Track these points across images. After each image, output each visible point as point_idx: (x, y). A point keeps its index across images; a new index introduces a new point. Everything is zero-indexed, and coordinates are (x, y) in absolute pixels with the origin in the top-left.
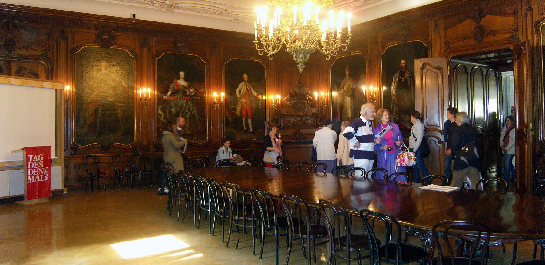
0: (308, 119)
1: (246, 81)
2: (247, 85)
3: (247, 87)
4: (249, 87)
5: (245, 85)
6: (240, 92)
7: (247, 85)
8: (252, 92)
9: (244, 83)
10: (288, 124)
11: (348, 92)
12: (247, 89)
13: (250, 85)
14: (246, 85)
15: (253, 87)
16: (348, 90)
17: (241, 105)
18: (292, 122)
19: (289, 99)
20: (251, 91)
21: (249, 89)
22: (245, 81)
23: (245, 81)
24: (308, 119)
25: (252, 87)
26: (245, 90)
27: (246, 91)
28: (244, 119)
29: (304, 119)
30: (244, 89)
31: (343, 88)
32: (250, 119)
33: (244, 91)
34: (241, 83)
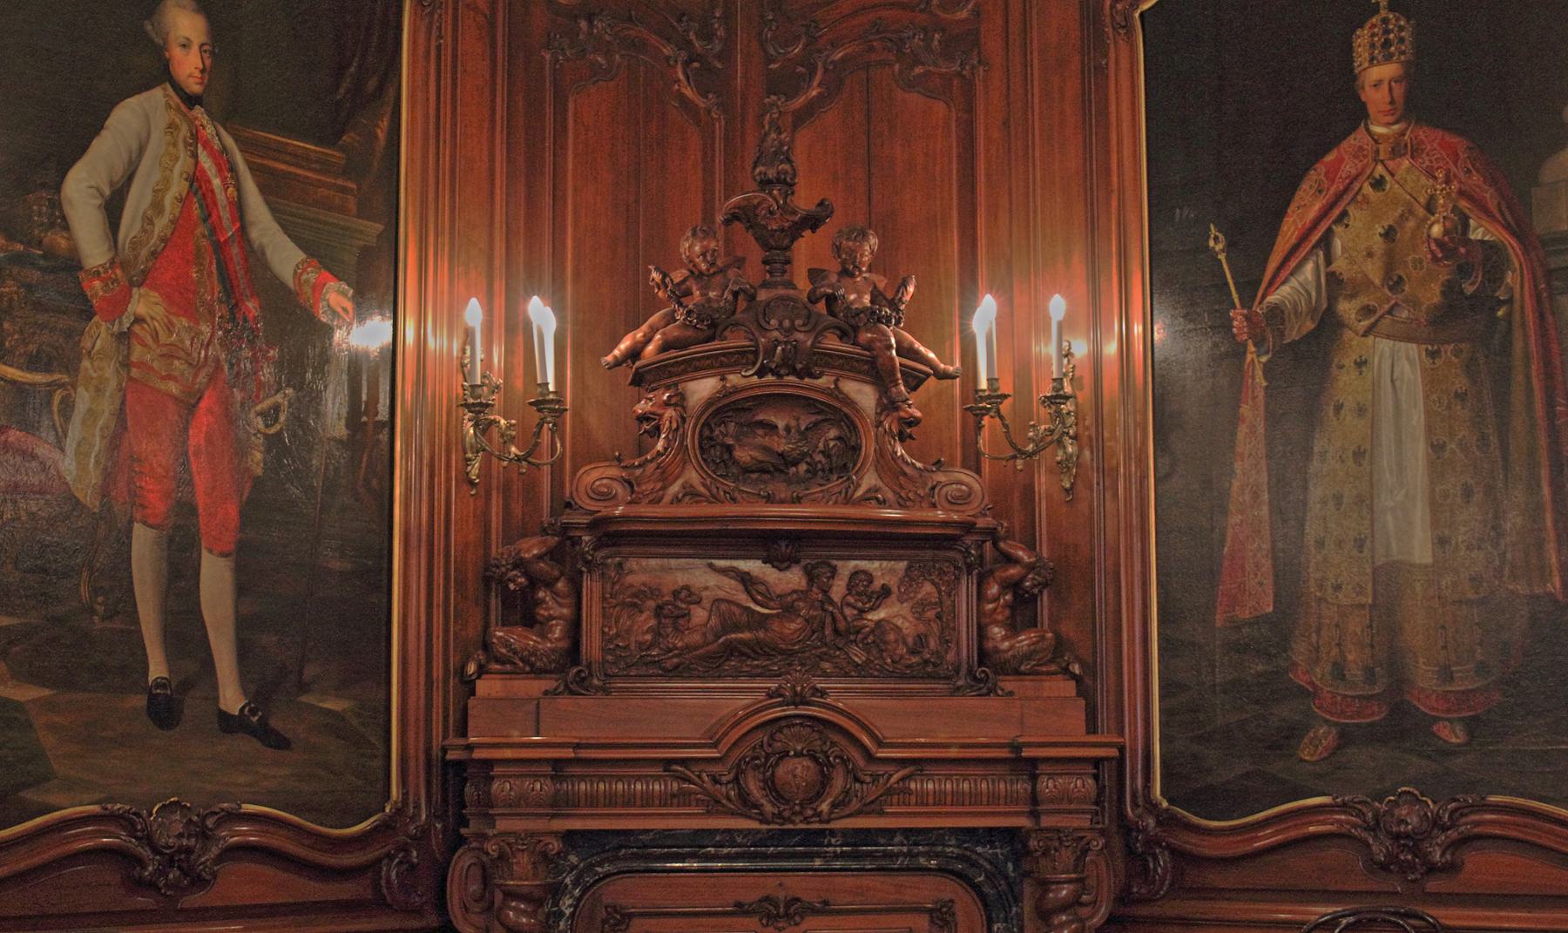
0: (886, 592)
1: (195, 88)
2: (196, 137)
3: (206, 162)
4: (227, 167)
5: (172, 126)
6: (113, 208)
7: (196, 137)
8: (254, 234)
9: (168, 106)
10: (657, 632)
11: (1396, 285)
12: (196, 180)
13: (230, 142)
14: (184, 130)
15: (271, 187)
16: (1390, 263)
17: (126, 364)
18: (699, 614)
19: (665, 347)
20: (239, 207)
21: (216, 182)
22: (177, 88)
23: (177, 88)
24: (886, 592)
25: (254, 169)
26: (178, 187)
27: (184, 201)
28: (144, 545)
29: (838, 590)
30: (166, 182)
31: (1326, 242)
32: (223, 555)
33: (157, 206)
34: (132, 102)
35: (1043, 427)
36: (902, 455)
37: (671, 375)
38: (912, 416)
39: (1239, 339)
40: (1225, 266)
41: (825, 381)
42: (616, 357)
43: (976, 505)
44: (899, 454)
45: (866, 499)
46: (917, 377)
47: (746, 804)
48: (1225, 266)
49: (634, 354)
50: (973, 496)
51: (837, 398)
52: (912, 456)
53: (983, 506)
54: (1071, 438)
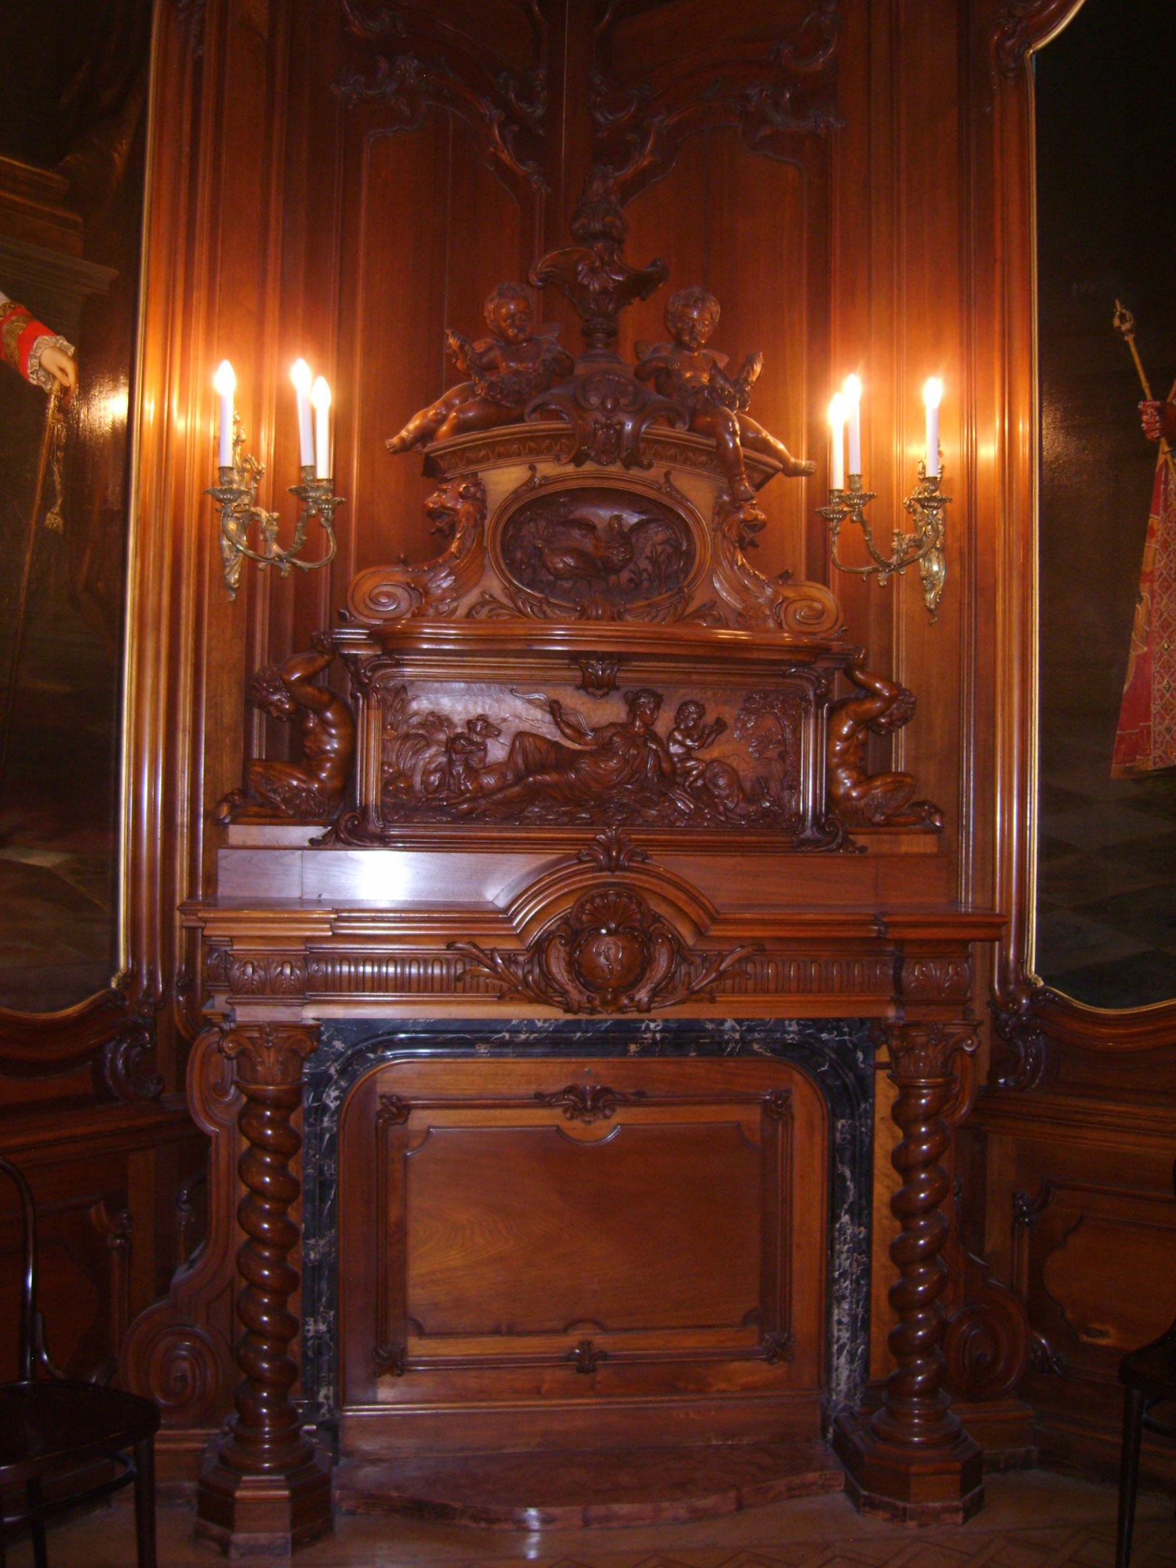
35: (908, 536)
36: (743, 564)
37: (470, 462)
38: (756, 519)
39: (1149, 436)
40: (1133, 349)
41: (656, 473)
42: (403, 440)
43: (829, 625)
44: (739, 563)
45: (699, 614)
46: (763, 472)
47: (543, 992)
48: (1133, 349)
49: (426, 434)
50: (825, 614)
51: (668, 494)
52: (755, 567)
53: (836, 628)
54: (937, 549)
